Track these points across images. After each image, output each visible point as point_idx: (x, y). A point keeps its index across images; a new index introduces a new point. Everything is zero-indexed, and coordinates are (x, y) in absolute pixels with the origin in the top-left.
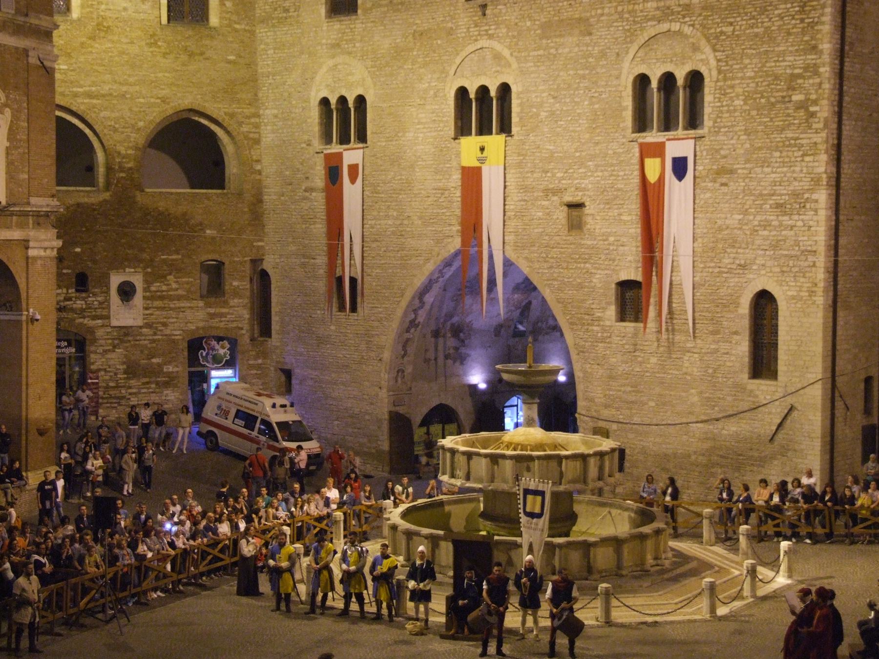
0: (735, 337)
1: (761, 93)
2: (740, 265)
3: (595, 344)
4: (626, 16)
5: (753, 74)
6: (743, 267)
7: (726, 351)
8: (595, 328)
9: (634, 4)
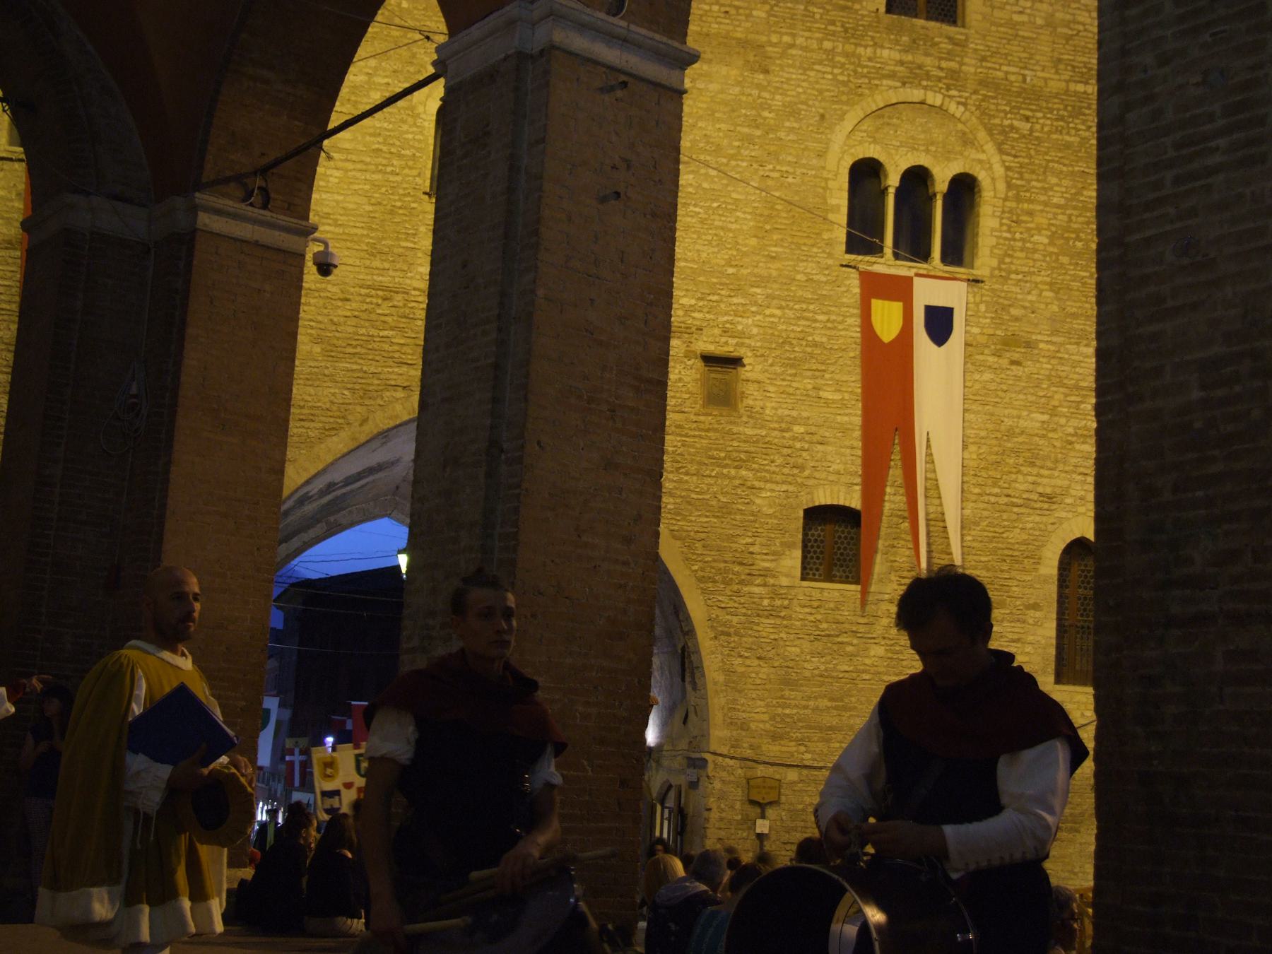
0: (1031, 613)
1: (1077, 231)
2: (1041, 494)
3: (756, 620)
4: (843, 60)
5: (1062, 202)
6: (1050, 498)
7: (1016, 637)
8: (756, 590)
9: (856, 45)
